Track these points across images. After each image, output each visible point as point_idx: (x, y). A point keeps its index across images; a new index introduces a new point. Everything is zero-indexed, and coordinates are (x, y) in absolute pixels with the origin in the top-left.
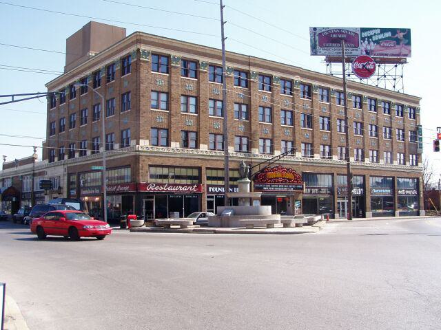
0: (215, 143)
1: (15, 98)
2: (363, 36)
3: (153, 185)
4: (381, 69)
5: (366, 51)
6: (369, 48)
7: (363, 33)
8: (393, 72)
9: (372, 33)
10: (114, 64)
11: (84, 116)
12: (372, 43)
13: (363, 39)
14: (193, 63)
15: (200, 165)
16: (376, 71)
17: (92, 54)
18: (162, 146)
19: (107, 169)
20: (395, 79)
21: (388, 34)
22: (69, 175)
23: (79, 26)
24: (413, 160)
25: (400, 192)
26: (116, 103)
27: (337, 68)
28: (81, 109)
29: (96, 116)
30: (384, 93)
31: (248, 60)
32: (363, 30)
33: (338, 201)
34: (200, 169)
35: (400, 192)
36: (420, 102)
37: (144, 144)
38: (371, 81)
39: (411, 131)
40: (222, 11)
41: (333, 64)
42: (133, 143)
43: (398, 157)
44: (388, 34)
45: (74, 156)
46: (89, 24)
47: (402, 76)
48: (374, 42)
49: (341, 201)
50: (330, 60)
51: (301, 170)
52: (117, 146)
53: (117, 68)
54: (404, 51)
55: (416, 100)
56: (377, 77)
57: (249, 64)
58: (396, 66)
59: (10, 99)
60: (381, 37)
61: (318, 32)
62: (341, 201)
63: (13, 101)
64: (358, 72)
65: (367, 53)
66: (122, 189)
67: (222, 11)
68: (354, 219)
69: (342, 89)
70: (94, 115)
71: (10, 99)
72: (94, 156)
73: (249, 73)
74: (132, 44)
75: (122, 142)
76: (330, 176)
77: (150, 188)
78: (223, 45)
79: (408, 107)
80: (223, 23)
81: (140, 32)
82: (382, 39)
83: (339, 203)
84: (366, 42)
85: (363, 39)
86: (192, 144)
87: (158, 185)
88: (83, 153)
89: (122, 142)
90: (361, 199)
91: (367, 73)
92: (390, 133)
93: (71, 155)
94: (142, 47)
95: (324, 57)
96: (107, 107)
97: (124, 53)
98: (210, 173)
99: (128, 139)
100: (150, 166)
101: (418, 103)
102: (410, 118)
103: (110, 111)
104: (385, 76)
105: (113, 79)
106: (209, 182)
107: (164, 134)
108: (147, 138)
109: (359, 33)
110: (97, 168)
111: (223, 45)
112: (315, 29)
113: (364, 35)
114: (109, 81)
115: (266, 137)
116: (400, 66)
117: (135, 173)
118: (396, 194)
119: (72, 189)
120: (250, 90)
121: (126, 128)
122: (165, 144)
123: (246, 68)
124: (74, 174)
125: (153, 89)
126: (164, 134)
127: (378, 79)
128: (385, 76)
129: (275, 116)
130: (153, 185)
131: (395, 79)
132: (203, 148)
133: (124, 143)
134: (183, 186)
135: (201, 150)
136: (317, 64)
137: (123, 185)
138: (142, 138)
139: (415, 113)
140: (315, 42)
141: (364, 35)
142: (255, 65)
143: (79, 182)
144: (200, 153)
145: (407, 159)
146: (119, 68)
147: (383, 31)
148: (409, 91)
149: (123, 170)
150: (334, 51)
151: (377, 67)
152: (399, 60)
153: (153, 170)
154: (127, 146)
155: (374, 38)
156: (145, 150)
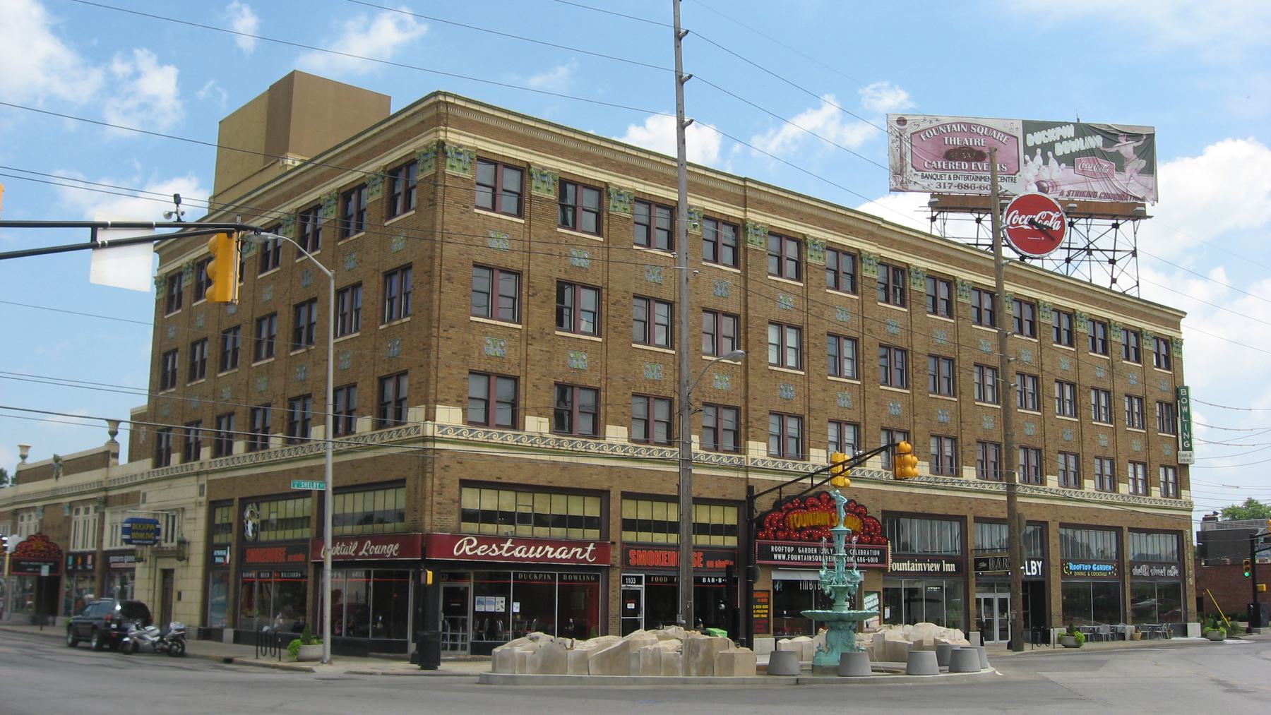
0: (647, 422)
1: (103, 237)
2: (1030, 144)
3: (470, 542)
4: (1078, 234)
5: (1038, 184)
6: (1046, 175)
7: (1029, 136)
8: (1105, 243)
9: (1053, 135)
10: (364, 186)
11: (264, 335)
12: (1053, 162)
13: (1030, 151)
14: (581, 192)
15: (605, 486)
16: (1066, 239)
17: (292, 161)
18: (499, 426)
19: (337, 490)
20: (1112, 262)
21: (1096, 141)
22: (213, 506)
23: (260, 87)
24: (1166, 482)
25: (1136, 571)
26: (370, 295)
27: (963, 228)
28: (258, 314)
29: (302, 334)
30: (1089, 292)
31: (741, 192)
32: (1030, 127)
33: (978, 596)
34: (602, 495)
35: (1136, 571)
36: (1183, 322)
37: (449, 416)
38: (1052, 262)
39: (1161, 403)
40: (678, 47)
41: (951, 215)
42: (415, 414)
43: (1162, 477)
44: (1096, 141)
45: (229, 452)
46: (291, 77)
47: (1134, 253)
48: (1060, 160)
49: (982, 596)
50: (942, 204)
51: (881, 506)
52: (364, 425)
53: (373, 197)
54: (1136, 190)
55: (1173, 318)
56: (1064, 254)
57: (744, 202)
58: (1116, 226)
59: (84, 235)
60: (1078, 145)
61: (910, 129)
62: (982, 596)
63: (94, 245)
64: (1018, 237)
65: (1041, 189)
66: (377, 550)
67: (678, 47)
68: (1028, 648)
69: (991, 282)
70: (297, 332)
71: (84, 235)
72: (293, 452)
73: (746, 231)
74: (423, 127)
75: (382, 413)
76: (956, 526)
77: (465, 549)
78: (682, 141)
79: (1150, 341)
80: (681, 81)
81: (445, 94)
82: (1081, 153)
83: (978, 601)
84: (1039, 159)
85: (1030, 151)
86: (584, 423)
87: (483, 539)
88: (257, 443)
89: (382, 413)
90: (1036, 591)
91: (1046, 240)
92: (1142, 413)
93: (223, 448)
94: (453, 137)
95: (926, 197)
96: (341, 314)
97: (395, 155)
98: (631, 510)
99: (399, 402)
100: (465, 483)
101: (1176, 326)
102: (1159, 365)
103: (345, 322)
104: (1090, 252)
105: (359, 228)
106: (630, 536)
107: (500, 401)
108: (458, 403)
109: (1020, 135)
110: (305, 485)
111: (682, 141)
112: (902, 121)
113: (1036, 138)
114: (345, 234)
115: (788, 410)
116: (1127, 226)
117: (417, 504)
118: (1127, 577)
119: (223, 547)
120: (745, 271)
121: (393, 370)
122: (509, 423)
123: (735, 212)
124: (227, 503)
125: (479, 259)
126: (500, 401)
127: (1068, 260)
128: (1090, 252)
129: (812, 351)
130: (470, 542)
131: (1112, 262)
132: (616, 434)
133: (389, 412)
134: (556, 544)
135: (608, 441)
136: (908, 210)
137: (378, 539)
138: (445, 402)
139: (1169, 353)
140: (902, 158)
141: (1036, 138)
142: (761, 205)
143: (243, 528)
144: (607, 451)
145: (1046, 466)
146: (378, 196)
147: (1083, 130)
148: (1153, 290)
149: (380, 494)
150: (955, 181)
151: (1067, 229)
152: (1128, 210)
153: (471, 500)
154: (396, 424)
155: (1060, 149)
156: (451, 435)
